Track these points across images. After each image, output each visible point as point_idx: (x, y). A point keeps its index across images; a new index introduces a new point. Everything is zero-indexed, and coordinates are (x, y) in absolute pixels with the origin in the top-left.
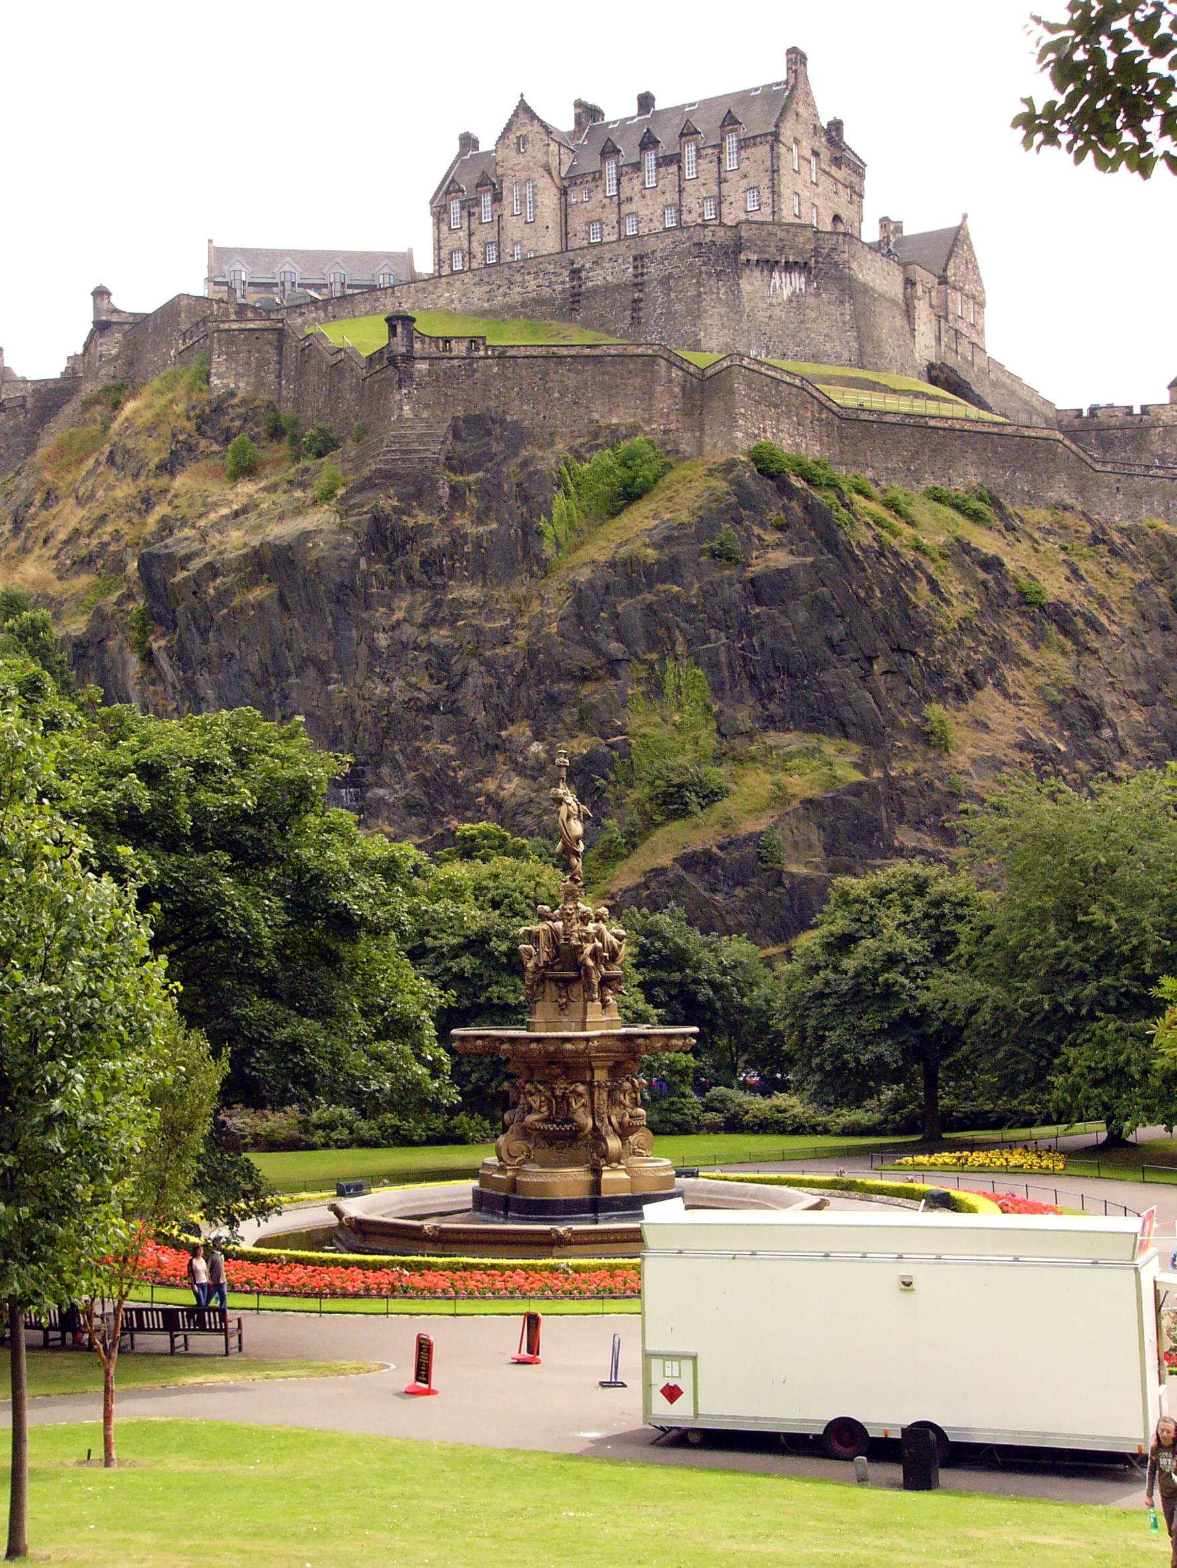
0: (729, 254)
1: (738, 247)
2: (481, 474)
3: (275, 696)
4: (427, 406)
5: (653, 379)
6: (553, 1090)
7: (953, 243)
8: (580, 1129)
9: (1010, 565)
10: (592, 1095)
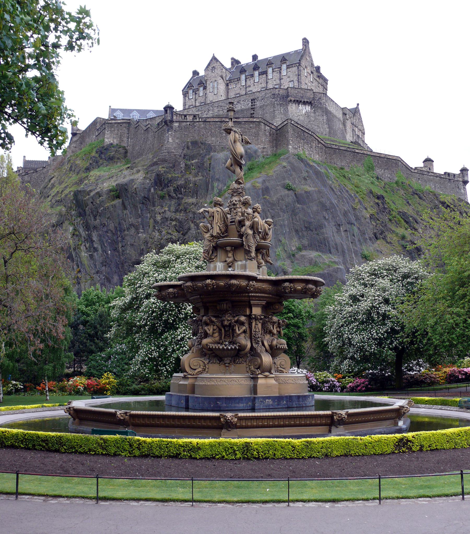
0: (286, 98)
1: (288, 96)
2: (197, 160)
3: (119, 238)
4: (178, 138)
6: (222, 322)
7: (356, 112)
8: (242, 348)
10: (250, 324)
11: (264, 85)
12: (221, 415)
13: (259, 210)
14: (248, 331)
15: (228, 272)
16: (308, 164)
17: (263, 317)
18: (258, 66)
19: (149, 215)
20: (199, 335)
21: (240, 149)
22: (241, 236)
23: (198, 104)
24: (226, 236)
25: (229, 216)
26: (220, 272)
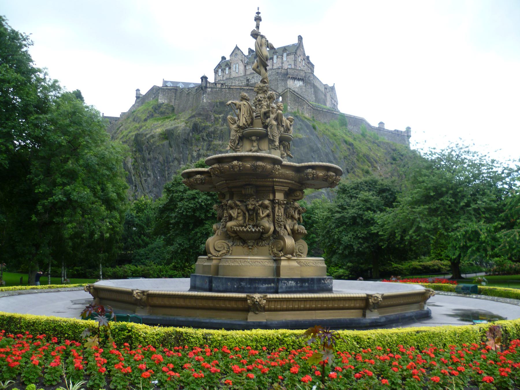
1: (287, 74)
3: (166, 168)
4: (210, 99)
6: (246, 206)
7: (333, 88)
9: (355, 145)
10: (273, 209)
12: (247, 296)
13: (281, 108)
17: (285, 202)
19: (188, 152)
20: (223, 218)
22: (266, 127)
23: (224, 79)
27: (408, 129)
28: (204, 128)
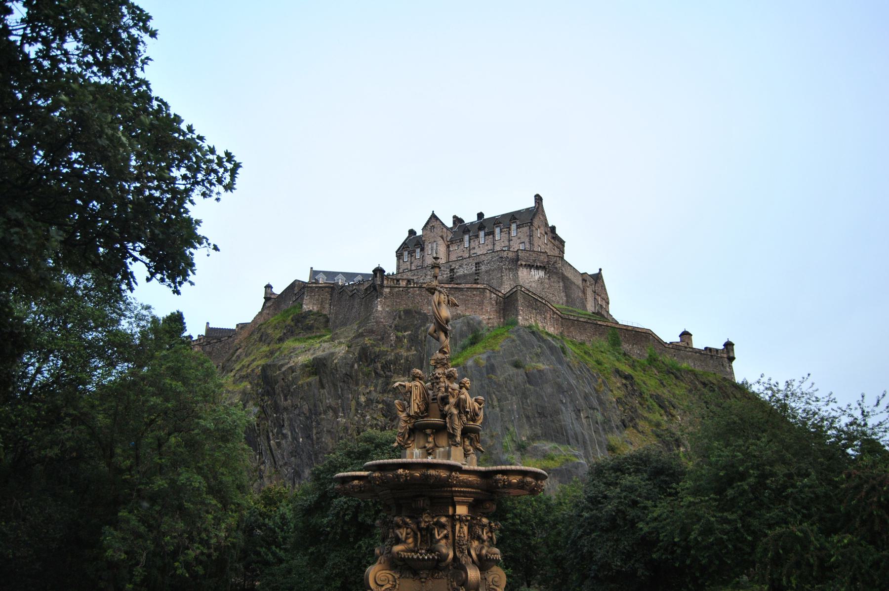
1: (518, 260)
3: (314, 423)
5: (485, 297)
6: (418, 523)
7: (597, 278)
8: (443, 558)
9: (636, 379)
11: (490, 247)
14: (450, 536)
15: (425, 460)
16: (542, 338)
17: (469, 518)
18: (484, 225)
21: (445, 312)
22: (444, 416)
23: (413, 268)
24: (426, 417)
25: (430, 392)
26: (414, 460)
27: (729, 345)
28: (378, 356)
